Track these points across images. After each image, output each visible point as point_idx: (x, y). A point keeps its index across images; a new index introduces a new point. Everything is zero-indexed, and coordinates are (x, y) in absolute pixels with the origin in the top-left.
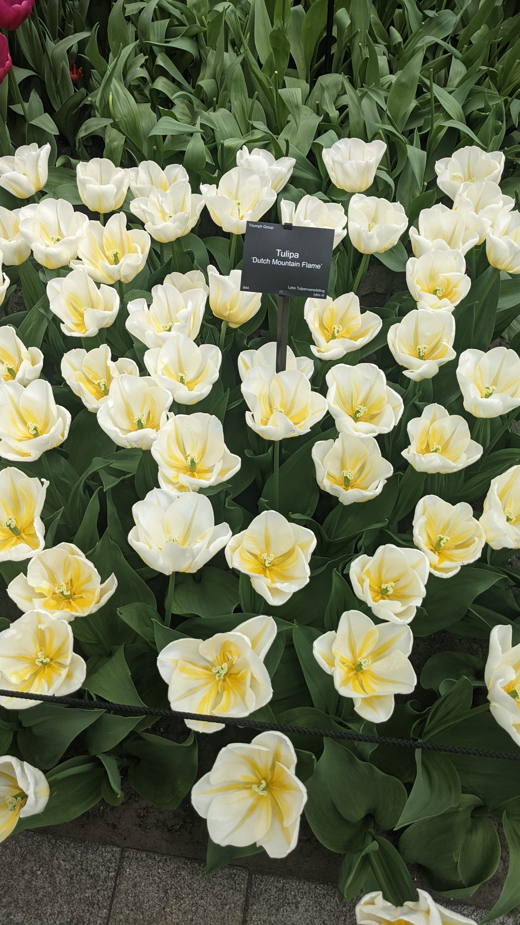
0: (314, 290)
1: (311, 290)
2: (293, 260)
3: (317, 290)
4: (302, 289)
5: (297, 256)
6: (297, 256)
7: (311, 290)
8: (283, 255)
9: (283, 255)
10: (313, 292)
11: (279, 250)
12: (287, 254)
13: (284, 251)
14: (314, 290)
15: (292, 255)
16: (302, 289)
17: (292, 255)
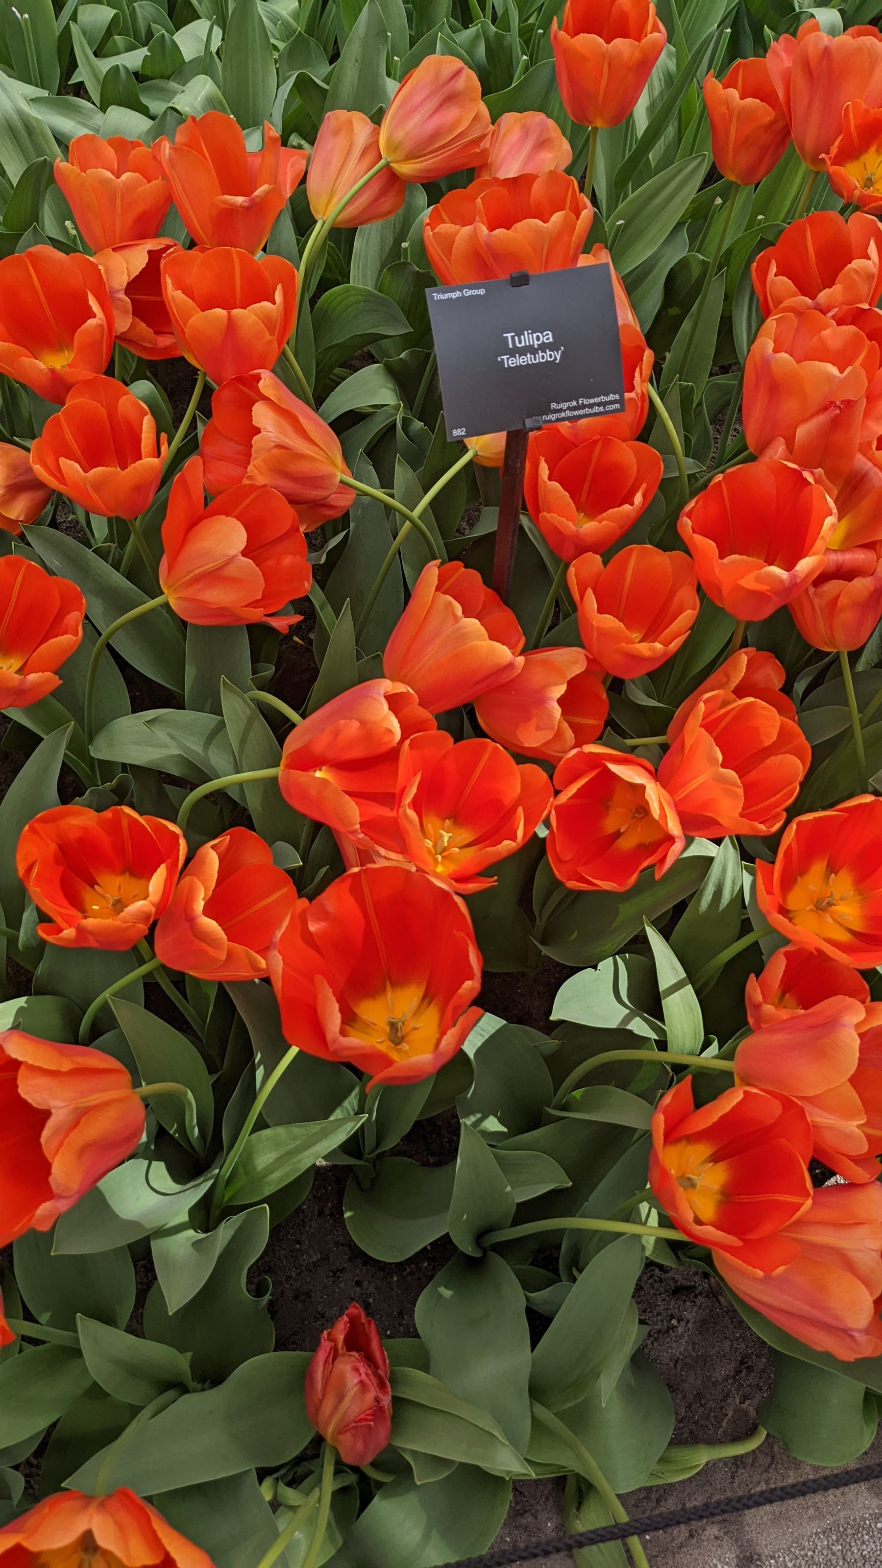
2: (543, 347)
5: (548, 337)
6: (548, 337)
8: (520, 342)
9: (520, 342)
11: (509, 335)
12: (529, 339)
13: (519, 334)
15: (538, 338)
17: (538, 338)
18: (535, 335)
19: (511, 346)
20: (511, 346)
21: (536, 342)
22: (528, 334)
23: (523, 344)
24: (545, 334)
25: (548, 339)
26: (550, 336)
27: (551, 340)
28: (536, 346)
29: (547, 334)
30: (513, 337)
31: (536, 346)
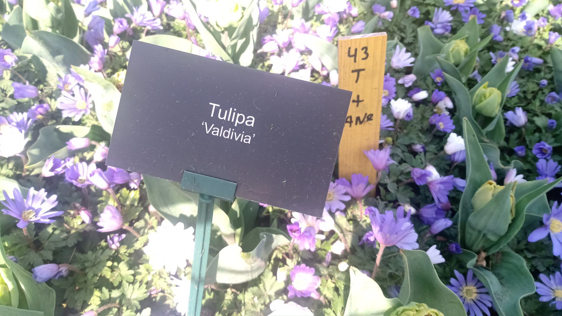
5: (251, 122)
6: (251, 122)
8: (222, 115)
9: (222, 115)
11: (214, 105)
13: (225, 107)
15: (240, 119)
17: (240, 119)
19: (212, 116)
20: (212, 116)
21: (237, 121)
24: (248, 118)
25: (249, 123)
26: (253, 121)
27: (252, 125)
28: (236, 125)
29: (252, 119)
31: (236, 125)
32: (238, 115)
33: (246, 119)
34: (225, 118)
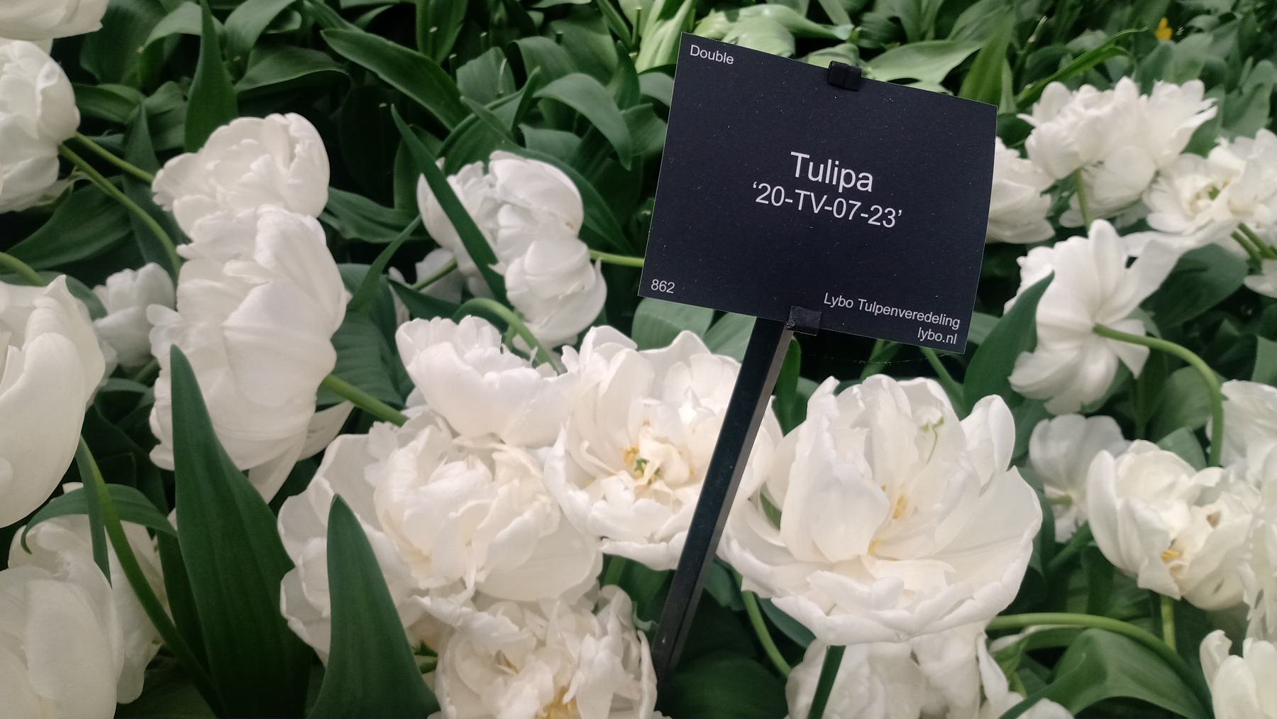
0: (921, 317)
1: (908, 314)
3: (932, 318)
4: (875, 309)
5: (867, 182)
7: (908, 314)
8: (815, 174)
9: (815, 174)
10: (915, 324)
11: (800, 156)
12: (831, 173)
13: (819, 159)
14: (921, 317)
15: (848, 178)
16: (875, 309)
17: (848, 178)
18: (844, 172)
21: (842, 183)
22: (833, 166)
23: (820, 178)
25: (863, 185)
26: (870, 182)
27: (869, 188)
30: (805, 162)
32: (844, 172)
33: (858, 179)
34: (820, 178)
